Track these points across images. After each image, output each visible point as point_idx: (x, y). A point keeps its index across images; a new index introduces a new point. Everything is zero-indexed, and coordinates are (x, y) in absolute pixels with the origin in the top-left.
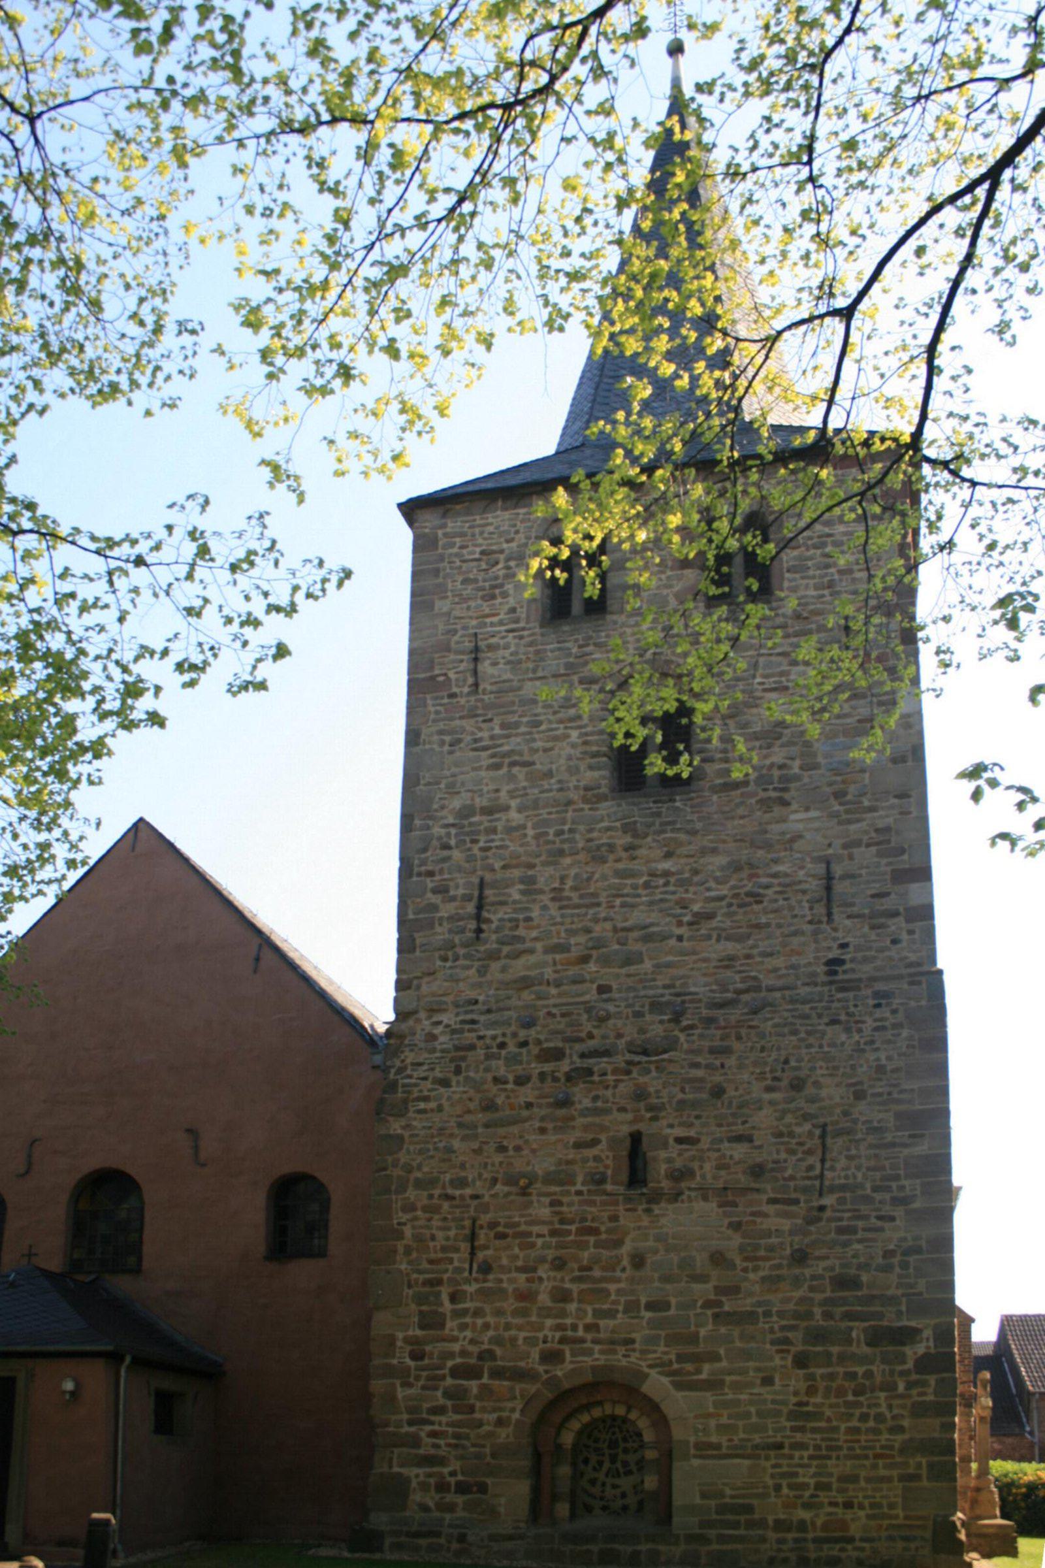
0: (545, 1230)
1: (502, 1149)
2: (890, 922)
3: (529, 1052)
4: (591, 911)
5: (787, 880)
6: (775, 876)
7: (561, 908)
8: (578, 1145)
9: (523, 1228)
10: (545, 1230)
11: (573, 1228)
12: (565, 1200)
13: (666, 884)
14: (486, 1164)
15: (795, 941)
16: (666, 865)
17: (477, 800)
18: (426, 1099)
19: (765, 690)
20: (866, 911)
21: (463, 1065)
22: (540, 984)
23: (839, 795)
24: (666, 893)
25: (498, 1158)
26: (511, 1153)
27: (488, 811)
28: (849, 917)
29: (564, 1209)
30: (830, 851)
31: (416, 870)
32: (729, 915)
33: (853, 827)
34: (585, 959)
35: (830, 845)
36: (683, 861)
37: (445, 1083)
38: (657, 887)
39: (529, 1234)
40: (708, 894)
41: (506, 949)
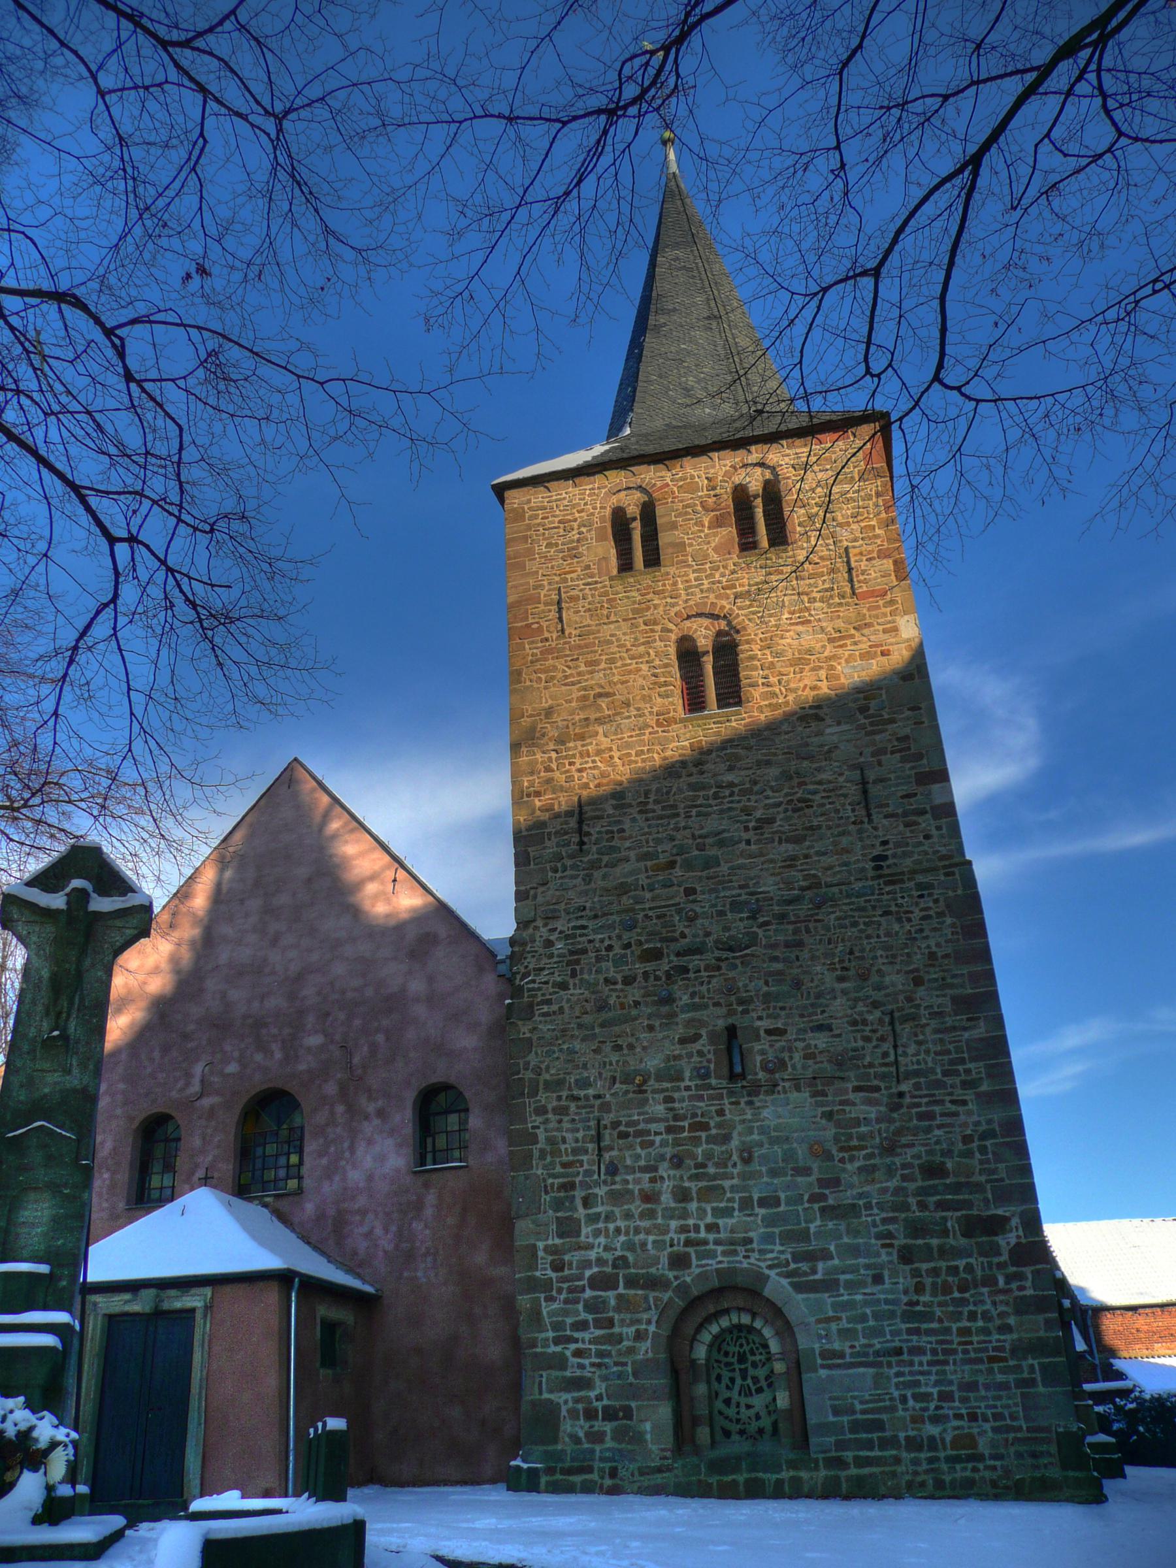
0: (661, 1127)
1: (618, 1048)
3: (632, 952)
4: (673, 821)
7: (647, 820)
8: (683, 1041)
9: (642, 1126)
10: (661, 1127)
11: (686, 1124)
12: (676, 1095)
13: (732, 794)
14: (605, 1063)
18: (548, 1002)
21: (577, 967)
24: (732, 802)
25: (614, 1058)
26: (625, 1052)
29: (676, 1105)
36: (743, 773)
37: (563, 986)
38: (724, 797)
39: (648, 1132)
40: (767, 801)
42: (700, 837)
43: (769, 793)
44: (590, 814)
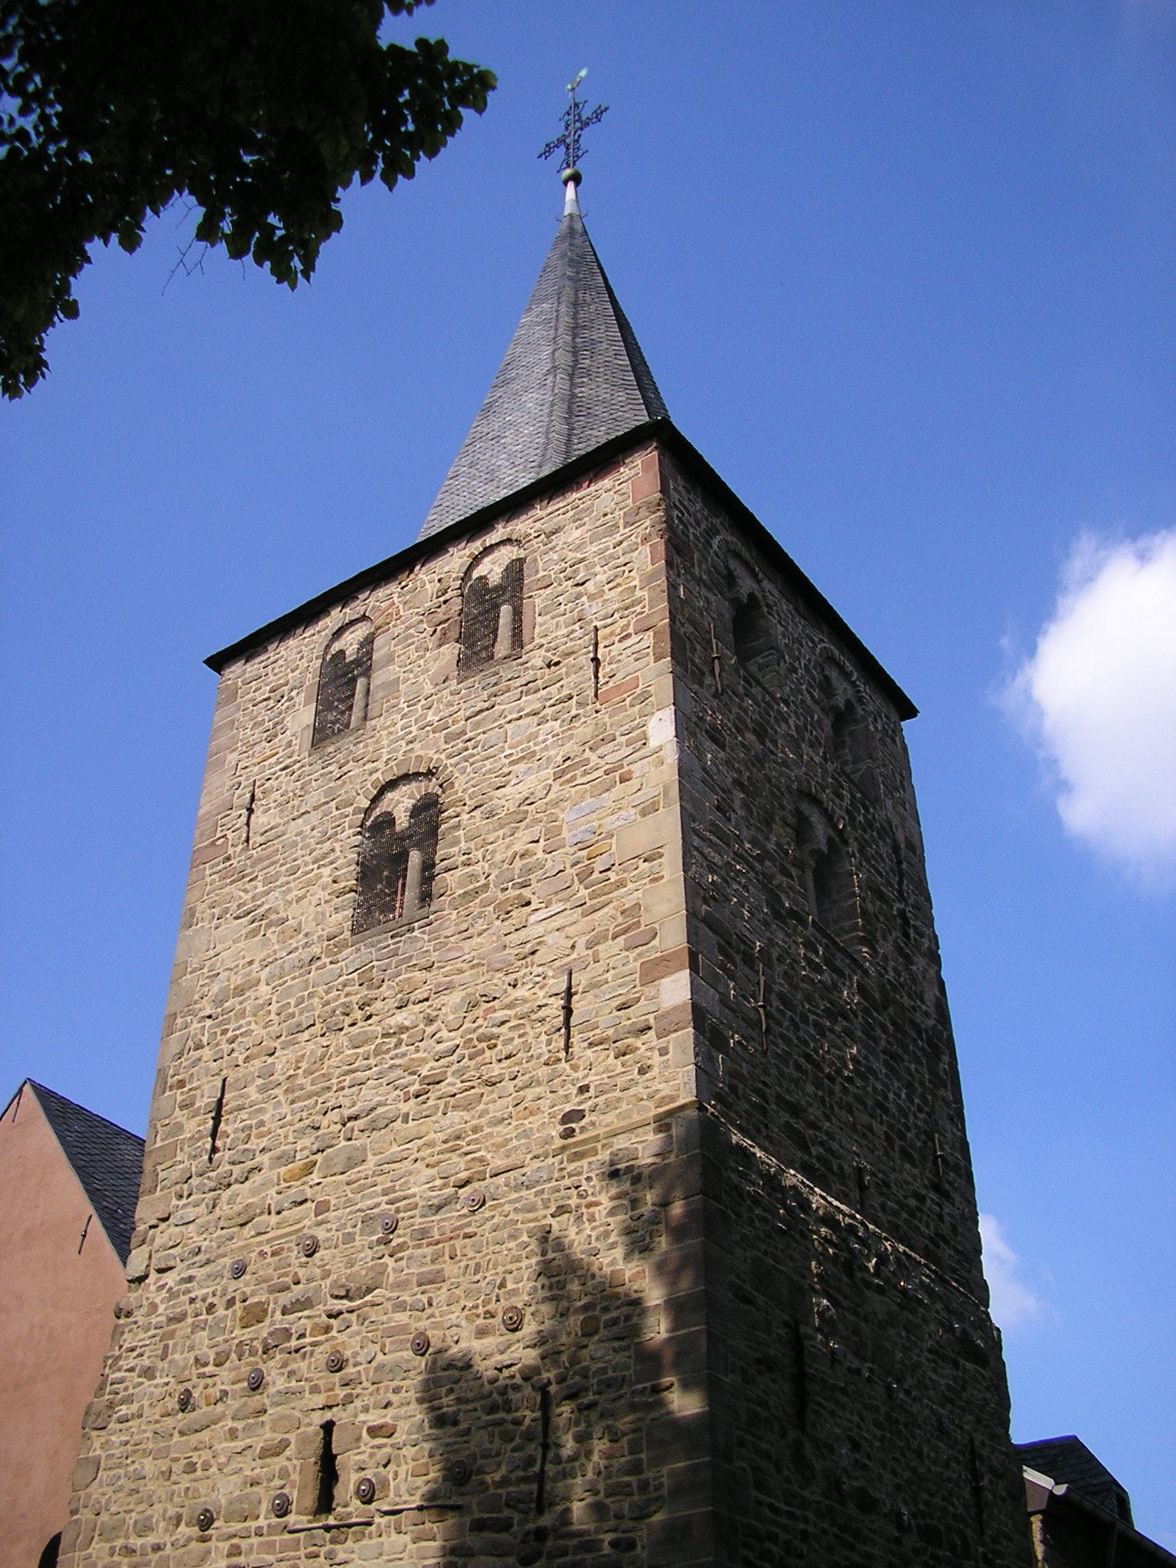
2: (638, 1043)
5: (526, 1008)
12: (244, 1544)
13: (398, 1045)
15: (530, 1093)
16: (401, 1018)
17: (233, 977)
19: (512, 763)
20: (610, 1032)
22: (262, 1213)
24: (396, 1056)
25: (185, 1482)
27: (240, 991)
30: (574, 956)
31: (170, 1081)
34: (309, 1168)
35: (573, 947)
36: (417, 1008)
38: (388, 1051)
41: (237, 1170)
42: (350, 1119)
43: (444, 1034)
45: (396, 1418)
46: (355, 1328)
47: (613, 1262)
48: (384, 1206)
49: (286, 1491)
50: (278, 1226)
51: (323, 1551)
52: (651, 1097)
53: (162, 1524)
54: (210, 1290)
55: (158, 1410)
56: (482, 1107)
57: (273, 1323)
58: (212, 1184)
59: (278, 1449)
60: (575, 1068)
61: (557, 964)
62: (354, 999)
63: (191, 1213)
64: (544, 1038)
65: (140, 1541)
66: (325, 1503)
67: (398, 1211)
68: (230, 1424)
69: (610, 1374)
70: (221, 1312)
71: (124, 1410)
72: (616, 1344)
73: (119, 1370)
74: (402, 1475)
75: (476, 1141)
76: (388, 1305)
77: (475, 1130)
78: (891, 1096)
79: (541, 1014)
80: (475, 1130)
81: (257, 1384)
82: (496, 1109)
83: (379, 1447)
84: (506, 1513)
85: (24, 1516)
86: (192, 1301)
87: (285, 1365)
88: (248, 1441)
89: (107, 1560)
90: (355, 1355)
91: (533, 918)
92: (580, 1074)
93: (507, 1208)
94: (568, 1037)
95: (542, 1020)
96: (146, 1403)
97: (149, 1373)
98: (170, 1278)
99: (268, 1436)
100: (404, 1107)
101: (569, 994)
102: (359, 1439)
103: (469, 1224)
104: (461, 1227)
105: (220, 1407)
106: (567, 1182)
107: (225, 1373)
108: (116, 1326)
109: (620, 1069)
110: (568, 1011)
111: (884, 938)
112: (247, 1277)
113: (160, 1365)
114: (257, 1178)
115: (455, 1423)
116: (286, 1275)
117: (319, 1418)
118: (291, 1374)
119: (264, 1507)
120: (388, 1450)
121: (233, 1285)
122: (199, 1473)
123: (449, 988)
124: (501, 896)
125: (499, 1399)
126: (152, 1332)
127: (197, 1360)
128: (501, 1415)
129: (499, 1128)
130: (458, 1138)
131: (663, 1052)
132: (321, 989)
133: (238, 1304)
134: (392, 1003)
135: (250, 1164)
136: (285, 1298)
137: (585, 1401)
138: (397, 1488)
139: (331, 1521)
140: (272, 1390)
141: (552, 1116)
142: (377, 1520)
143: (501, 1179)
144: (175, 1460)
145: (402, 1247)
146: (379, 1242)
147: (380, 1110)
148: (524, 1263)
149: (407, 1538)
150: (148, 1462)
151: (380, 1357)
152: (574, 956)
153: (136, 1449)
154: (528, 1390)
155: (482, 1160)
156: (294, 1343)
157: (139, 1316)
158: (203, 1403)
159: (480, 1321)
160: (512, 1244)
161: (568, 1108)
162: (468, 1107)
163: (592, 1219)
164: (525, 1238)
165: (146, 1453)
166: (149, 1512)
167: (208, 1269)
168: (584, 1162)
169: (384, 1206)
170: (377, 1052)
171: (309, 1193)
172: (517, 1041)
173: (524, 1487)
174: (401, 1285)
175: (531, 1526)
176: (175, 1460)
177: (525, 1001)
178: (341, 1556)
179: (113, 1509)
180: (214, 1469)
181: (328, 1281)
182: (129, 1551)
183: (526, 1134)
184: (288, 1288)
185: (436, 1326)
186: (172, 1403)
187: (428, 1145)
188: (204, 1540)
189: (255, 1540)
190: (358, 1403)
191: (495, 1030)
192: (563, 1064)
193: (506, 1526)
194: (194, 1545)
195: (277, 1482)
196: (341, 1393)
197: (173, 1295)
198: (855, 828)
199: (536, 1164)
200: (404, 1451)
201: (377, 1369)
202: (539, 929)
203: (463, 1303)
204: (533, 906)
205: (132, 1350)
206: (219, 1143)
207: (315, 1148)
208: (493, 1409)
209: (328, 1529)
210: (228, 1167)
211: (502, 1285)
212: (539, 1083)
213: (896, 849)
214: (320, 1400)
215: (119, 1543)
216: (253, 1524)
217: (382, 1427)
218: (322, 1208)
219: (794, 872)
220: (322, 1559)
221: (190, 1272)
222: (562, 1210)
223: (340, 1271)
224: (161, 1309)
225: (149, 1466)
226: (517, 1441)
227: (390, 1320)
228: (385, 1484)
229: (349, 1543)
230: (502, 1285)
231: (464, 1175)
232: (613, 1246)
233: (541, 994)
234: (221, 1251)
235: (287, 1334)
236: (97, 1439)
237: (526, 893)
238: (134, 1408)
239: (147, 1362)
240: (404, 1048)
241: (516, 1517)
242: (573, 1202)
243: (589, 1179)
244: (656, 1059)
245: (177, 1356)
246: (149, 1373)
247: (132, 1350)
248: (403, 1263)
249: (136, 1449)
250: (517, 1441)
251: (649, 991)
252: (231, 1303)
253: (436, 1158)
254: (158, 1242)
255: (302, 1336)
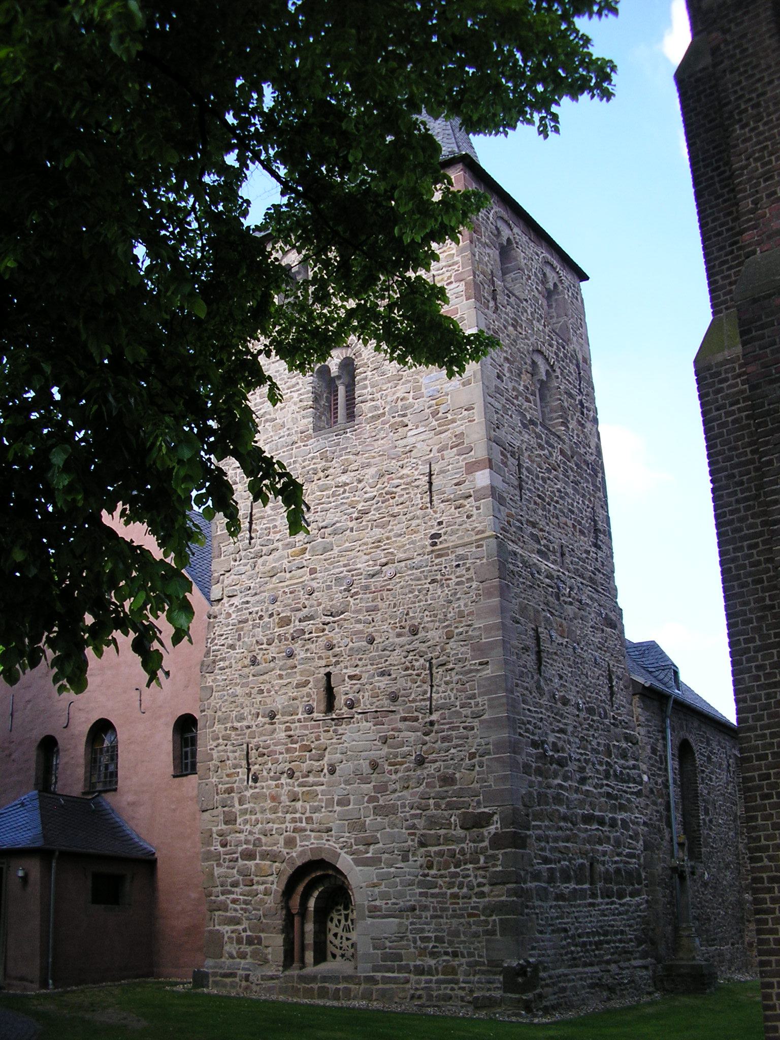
2: (465, 502)
5: (409, 480)
6: (401, 478)
8: (298, 686)
12: (293, 726)
13: (344, 492)
15: (414, 523)
16: (344, 478)
20: (452, 496)
23: (435, 414)
25: (259, 698)
28: (442, 502)
30: (431, 455)
32: (377, 509)
33: (443, 436)
34: (304, 551)
36: (353, 474)
41: (265, 549)
43: (368, 489)
44: (258, 515)
45: (362, 672)
46: (337, 630)
47: (459, 607)
48: (345, 573)
49: (310, 703)
50: (291, 579)
51: (331, 729)
52: (473, 530)
53: (249, 717)
54: (259, 608)
55: (240, 664)
56: (390, 527)
57: (295, 626)
58: (252, 555)
59: (306, 683)
60: (435, 512)
61: (423, 458)
62: (319, 466)
63: (243, 569)
64: (419, 496)
65: (239, 724)
66: (330, 706)
67: (353, 576)
68: (279, 672)
69: (460, 656)
70: (266, 619)
71: (222, 664)
72: (462, 643)
73: (216, 644)
74: (366, 697)
75: (388, 544)
76: (353, 620)
77: (388, 538)
78: (575, 504)
79: (416, 483)
80: (388, 538)
81: (291, 655)
82: (397, 529)
83: (354, 684)
84: (416, 714)
85: (160, 707)
86: (250, 613)
87: (303, 646)
88: (289, 680)
89: (224, 733)
90: (339, 643)
91: (410, 434)
92: (438, 515)
93: (407, 578)
94: (431, 497)
95: (418, 487)
96: (233, 661)
97: (232, 647)
98: (235, 601)
99: (298, 678)
100: (351, 524)
101: (430, 475)
102: (344, 680)
103: (389, 584)
104: (385, 586)
105: (272, 664)
106: (435, 568)
107: (272, 648)
108: (209, 623)
109: (457, 515)
110: (430, 483)
111: (572, 419)
112: (278, 603)
113: (238, 643)
114: (276, 554)
115: (390, 675)
116: (298, 603)
117: (324, 671)
118: (307, 650)
119: (300, 710)
120: (358, 686)
121: (271, 607)
122: (265, 694)
123: (368, 465)
124: (392, 421)
125: (409, 665)
126: (231, 627)
127: (257, 642)
128: (410, 672)
129: (399, 539)
130: (379, 542)
131: (478, 508)
132: (300, 459)
133: (275, 616)
134: (339, 470)
135: (271, 547)
136: (300, 615)
137: (449, 667)
138: (364, 703)
139: (334, 716)
140: (298, 657)
141: (425, 534)
142: (356, 716)
143: (403, 564)
144: (253, 688)
145: (356, 593)
146: (345, 590)
147: (338, 525)
148: (417, 605)
149: (371, 724)
150: (238, 688)
151: (351, 644)
152: (431, 455)
153: (232, 682)
154: (422, 661)
155: (392, 553)
156: (307, 636)
157: (221, 618)
158: (263, 662)
159: (398, 630)
160: (410, 595)
161: (433, 532)
162: (383, 527)
163: (448, 586)
164: (417, 593)
165: (237, 684)
166: (242, 711)
167: (257, 598)
168: (443, 559)
169: (345, 573)
170: (334, 495)
171: (305, 563)
172: (406, 496)
173: (423, 703)
174: (358, 611)
175: (428, 720)
176: (253, 688)
177: (408, 476)
178: (340, 732)
179: (223, 710)
180: (273, 692)
181: (321, 607)
182: (234, 729)
183: (413, 542)
184: (300, 610)
185: (377, 631)
186: (247, 662)
187: (365, 544)
188: (272, 724)
189: (297, 724)
190: (342, 665)
191: (394, 490)
192: (429, 510)
193: (416, 719)
194: (267, 726)
195: (306, 699)
196: (334, 660)
197: (239, 610)
198: (559, 362)
199: (419, 558)
200: (366, 686)
201: (350, 650)
202: (413, 440)
203: (389, 621)
204: (409, 428)
205: (222, 635)
206: (253, 535)
207: (306, 541)
208: (407, 669)
209: (333, 719)
210: (260, 547)
211: (407, 614)
212: (418, 518)
213: (578, 366)
214: (323, 663)
215: (229, 725)
216: (296, 717)
217: (355, 676)
218: (313, 571)
219: (531, 398)
220: (331, 732)
221: (247, 599)
222: (433, 581)
223: (326, 604)
224: (234, 616)
225: (239, 690)
226: (419, 683)
227: (354, 627)
228: (359, 701)
229: (344, 726)
230: (407, 614)
231: (384, 560)
232: (459, 599)
233: (416, 473)
234: (262, 589)
235: (303, 632)
236: (210, 679)
237: (405, 420)
238: (227, 663)
239: (231, 642)
240: (347, 495)
241: (420, 716)
242: (439, 577)
243: (445, 567)
244: (475, 512)
245: (246, 639)
246: (232, 647)
247: (222, 635)
248: (358, 601)
249: (232, 682)
250: (419, 683)
251: (470, 477)
252: (271, 615)
253: (369, 551)
254: (226, 582)
255: (311, 633)
